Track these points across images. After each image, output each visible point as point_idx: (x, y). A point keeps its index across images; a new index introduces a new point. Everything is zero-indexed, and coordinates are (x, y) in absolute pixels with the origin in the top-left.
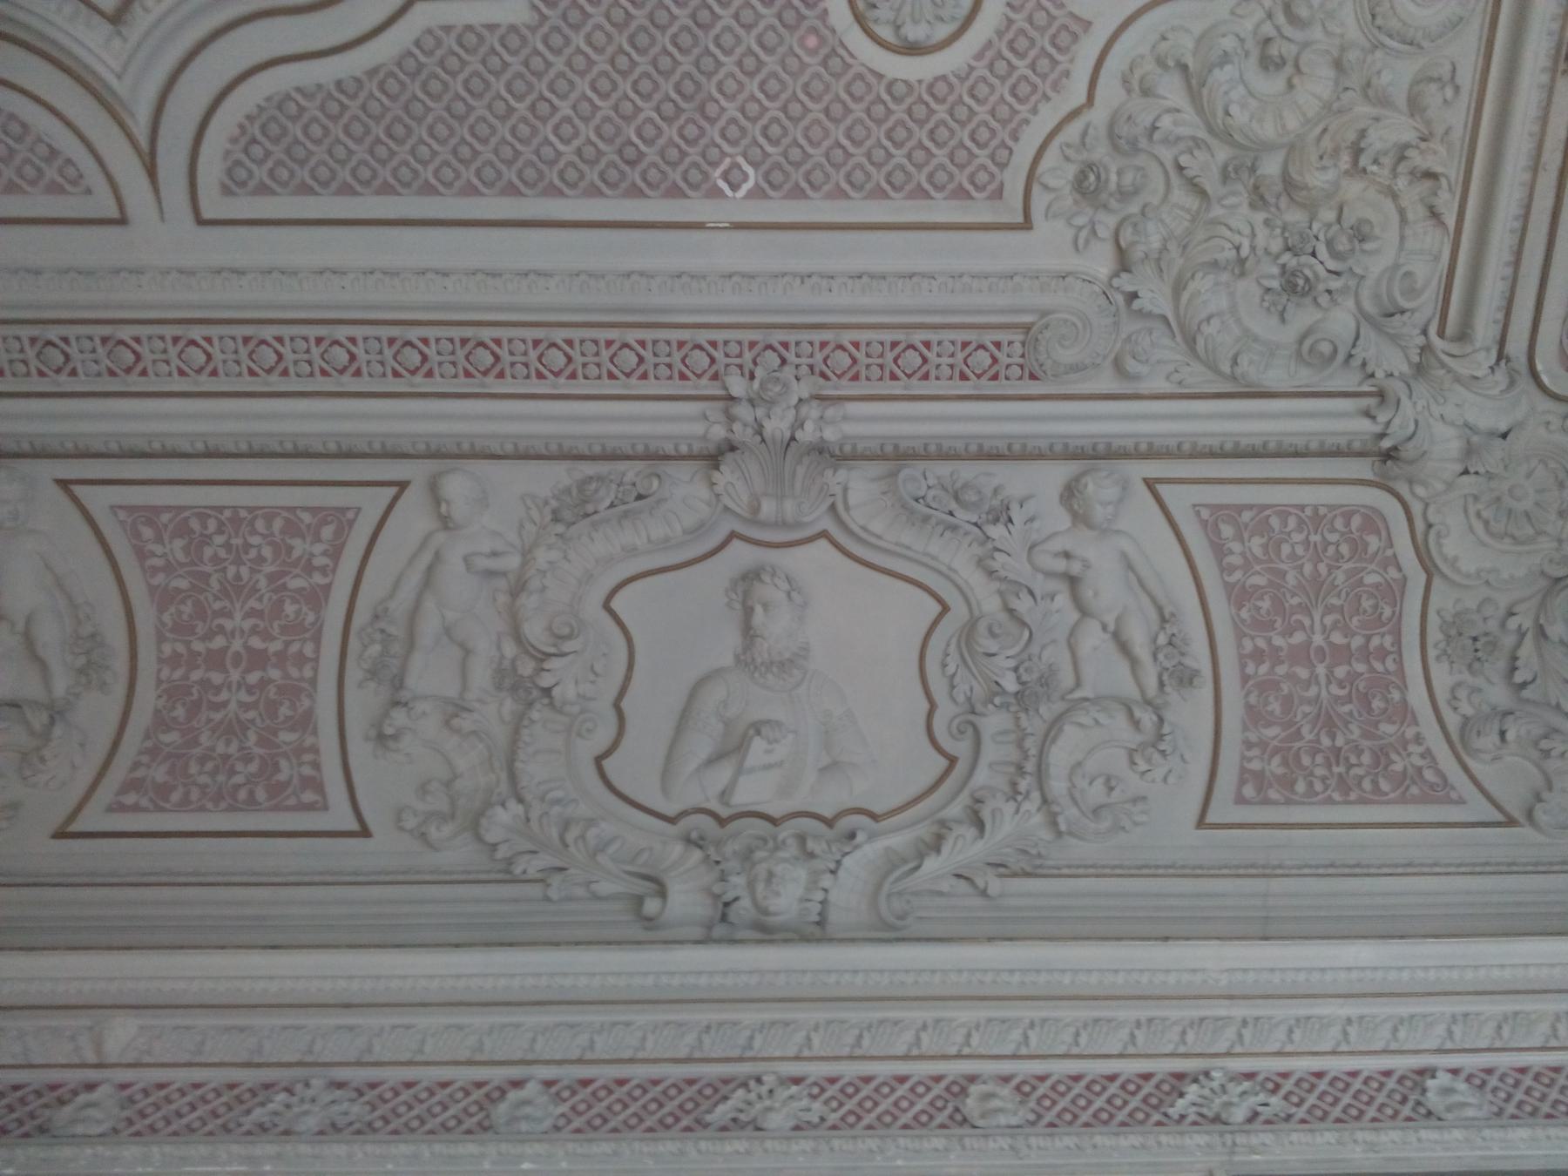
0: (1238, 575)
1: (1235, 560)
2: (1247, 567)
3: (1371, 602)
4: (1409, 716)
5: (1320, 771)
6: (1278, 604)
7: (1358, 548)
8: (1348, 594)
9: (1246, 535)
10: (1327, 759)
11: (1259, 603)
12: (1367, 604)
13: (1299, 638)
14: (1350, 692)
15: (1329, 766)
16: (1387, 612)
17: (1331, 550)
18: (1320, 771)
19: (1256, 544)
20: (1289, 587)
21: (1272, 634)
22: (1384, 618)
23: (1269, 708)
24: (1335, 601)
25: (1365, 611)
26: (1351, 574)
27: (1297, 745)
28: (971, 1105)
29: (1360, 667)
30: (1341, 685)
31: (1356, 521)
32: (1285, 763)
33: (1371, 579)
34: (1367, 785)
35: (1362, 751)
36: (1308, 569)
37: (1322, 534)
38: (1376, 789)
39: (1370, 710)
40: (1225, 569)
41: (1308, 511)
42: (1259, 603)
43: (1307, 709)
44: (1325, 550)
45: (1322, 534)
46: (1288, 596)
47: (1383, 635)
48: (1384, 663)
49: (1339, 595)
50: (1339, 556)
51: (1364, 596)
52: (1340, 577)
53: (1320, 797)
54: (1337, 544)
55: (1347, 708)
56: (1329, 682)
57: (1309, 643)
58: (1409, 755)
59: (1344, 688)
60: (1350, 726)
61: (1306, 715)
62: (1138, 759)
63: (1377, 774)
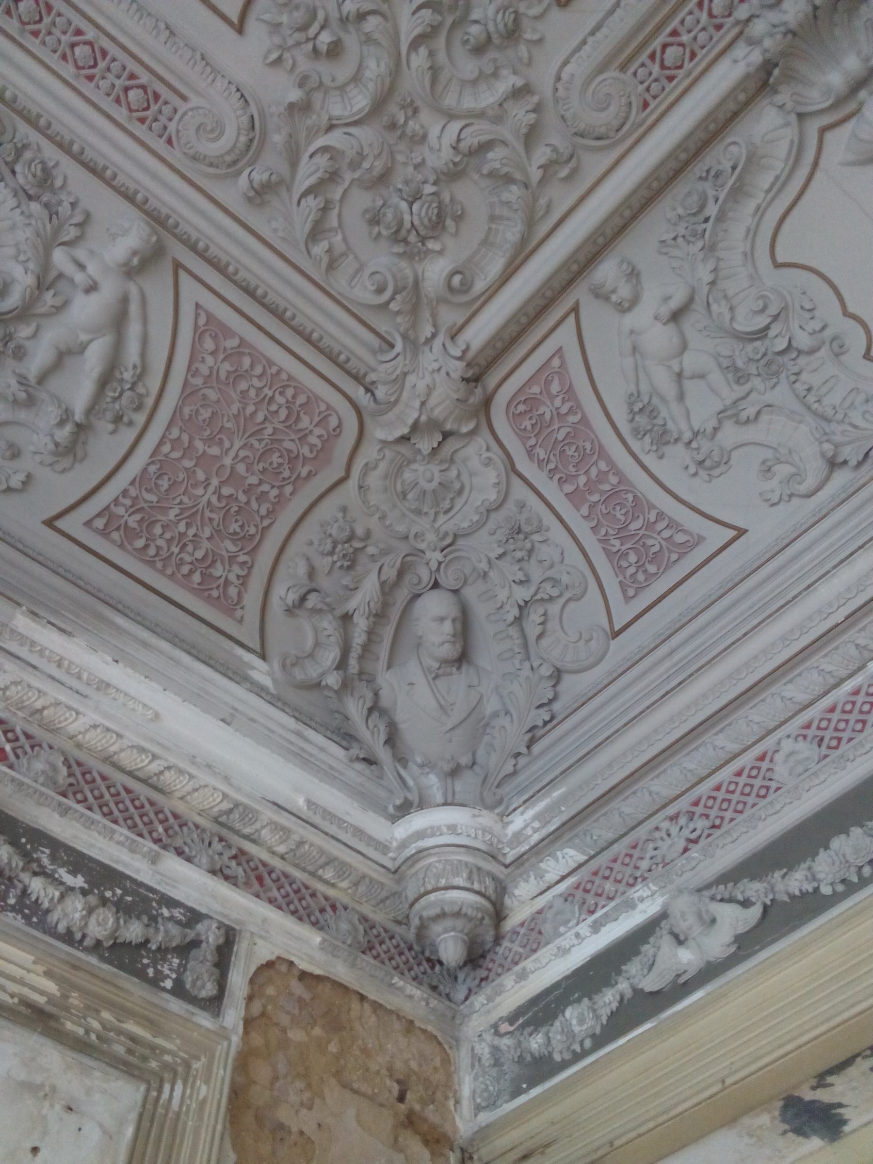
0: (242, 558)
1: (236, 569)
2: (232, 559)
3: (160, 482)
4: (188, 391)
5: (280, 400)
8: (174, 499)
9: (222, 581)
10: (269, 403)
11: (238, 530)
12: (165, 484)
13: (226, 491)
14: (218, 433)
15: (272, 399)
17: (168, 535)
18: (280, 400)
19: (218, 571)
20: (211, 528)
22: (158, 466)
23: (280, 460)
24: (185, 499)
25: (169, 479)
26: (164, 510)
27: (280, 426)
29: (199, 445)
31: (140, 543)
32: (298, 419)
33: (152, 498)
34: (258, 370)
35: (241, 392)
36: (191, 532)
37: (169, 550)
40: (249, 567)
41: (169, 571)
42: (238, 530)
43: (256, 444)
44: (172, 538)
45: (169, 550)
46: (215, 523)
47: (166, 455)
48: (179, 438)
49: (181, 503)
50: (165, 527)
51: (163, 489)
52: (172, 514)
53: (293, 384)
54: (161, 536)
55: (228, 425)
56: (228, 450)
57: (222, 483)
58: (211, 368)
60: (235, 412)
61: (260, 441)
63: (246, 371)
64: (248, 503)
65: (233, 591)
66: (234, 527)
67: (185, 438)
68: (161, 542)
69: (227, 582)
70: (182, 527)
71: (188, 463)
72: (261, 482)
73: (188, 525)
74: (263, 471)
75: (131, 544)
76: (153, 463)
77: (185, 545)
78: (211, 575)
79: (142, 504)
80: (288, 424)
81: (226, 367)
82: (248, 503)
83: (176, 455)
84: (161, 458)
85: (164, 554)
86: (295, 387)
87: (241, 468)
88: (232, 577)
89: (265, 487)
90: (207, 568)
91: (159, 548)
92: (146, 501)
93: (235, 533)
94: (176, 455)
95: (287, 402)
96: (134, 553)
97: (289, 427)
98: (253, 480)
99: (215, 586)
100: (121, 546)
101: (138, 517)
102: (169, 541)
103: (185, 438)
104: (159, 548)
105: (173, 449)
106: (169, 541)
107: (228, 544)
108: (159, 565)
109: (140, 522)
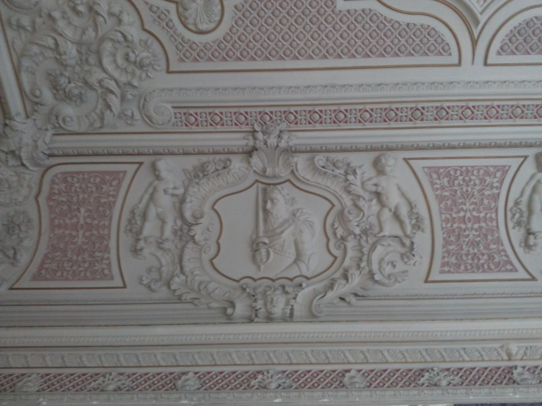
6: (454, 202)
7: (482, 181)
9: (441, 177)
12: (486, 202)
16: (493, 205)
18: (470, 262)
21: (452, 213)
28: (346, 380)
29: (483, 224)
30: (476, 230)
31: (482, 172)
34: (486, 266)
38: (489, 267)
39: (487, 239)
47: (492, 213)
50: (475, 185)
59: (477, 232)
62: (405, 257)
63: (489, 263)
64: (451, 215)
65: (435, 176)
66: (449, 202)
67: (490, 224)
68: (473, 178)
69: (439, 178)
70: (469, 189)
71: (482, 215)
72: (452, 226)
73: (467, 191)
74: (454, 231)
75: (485, 170)
76: (494, 207)
77: (464, 182)
78: (447, 177)
79: (488, 188)
80: (460, 255)
81: (497, 260)
82: (451, 215)
83: (488, 215)
84: (493, 211)
85: (470, 174)
86: (468, 270)
87: (463, 226)
88: (438, 182)
89: (449, 225)
90: (451, 178)
91: (473, 175)
92: (488, 190)
93: (448, 200)
94: (488, 215)
95: (467, 263)
96: (481, 167)
97: (458, 254)
98: (455, 225)
99: (443, 174)
100: (487, 167)
101: (487, 182)
102: (471, 180)
103: (490, 224)
104: (473, 175)
105: (491, 217)
106: (471, 180)
107: (447, 194)
108: (470, 168)
109: (485, 180)
